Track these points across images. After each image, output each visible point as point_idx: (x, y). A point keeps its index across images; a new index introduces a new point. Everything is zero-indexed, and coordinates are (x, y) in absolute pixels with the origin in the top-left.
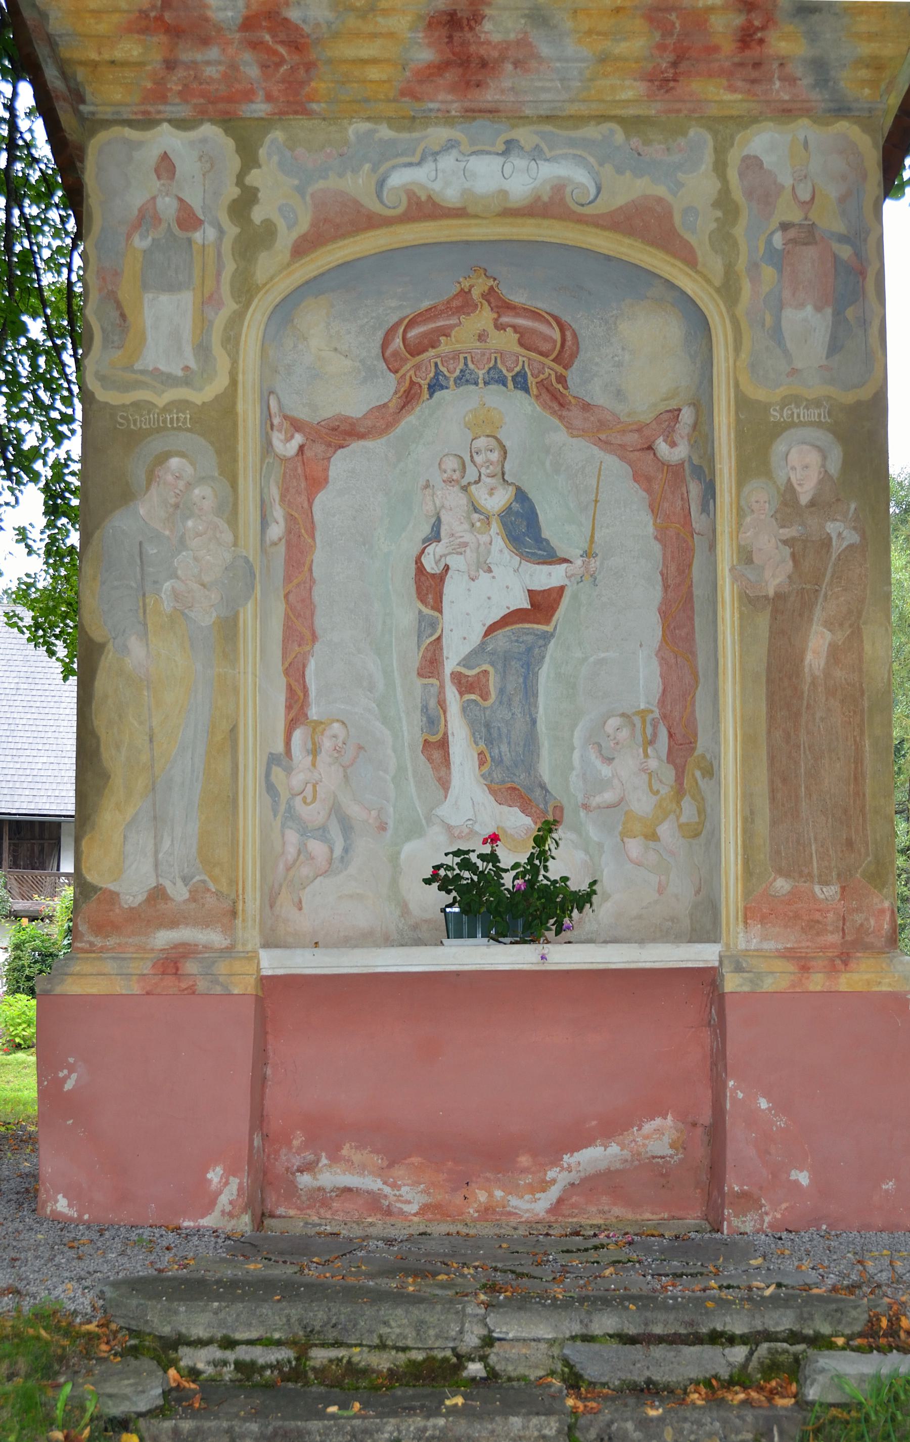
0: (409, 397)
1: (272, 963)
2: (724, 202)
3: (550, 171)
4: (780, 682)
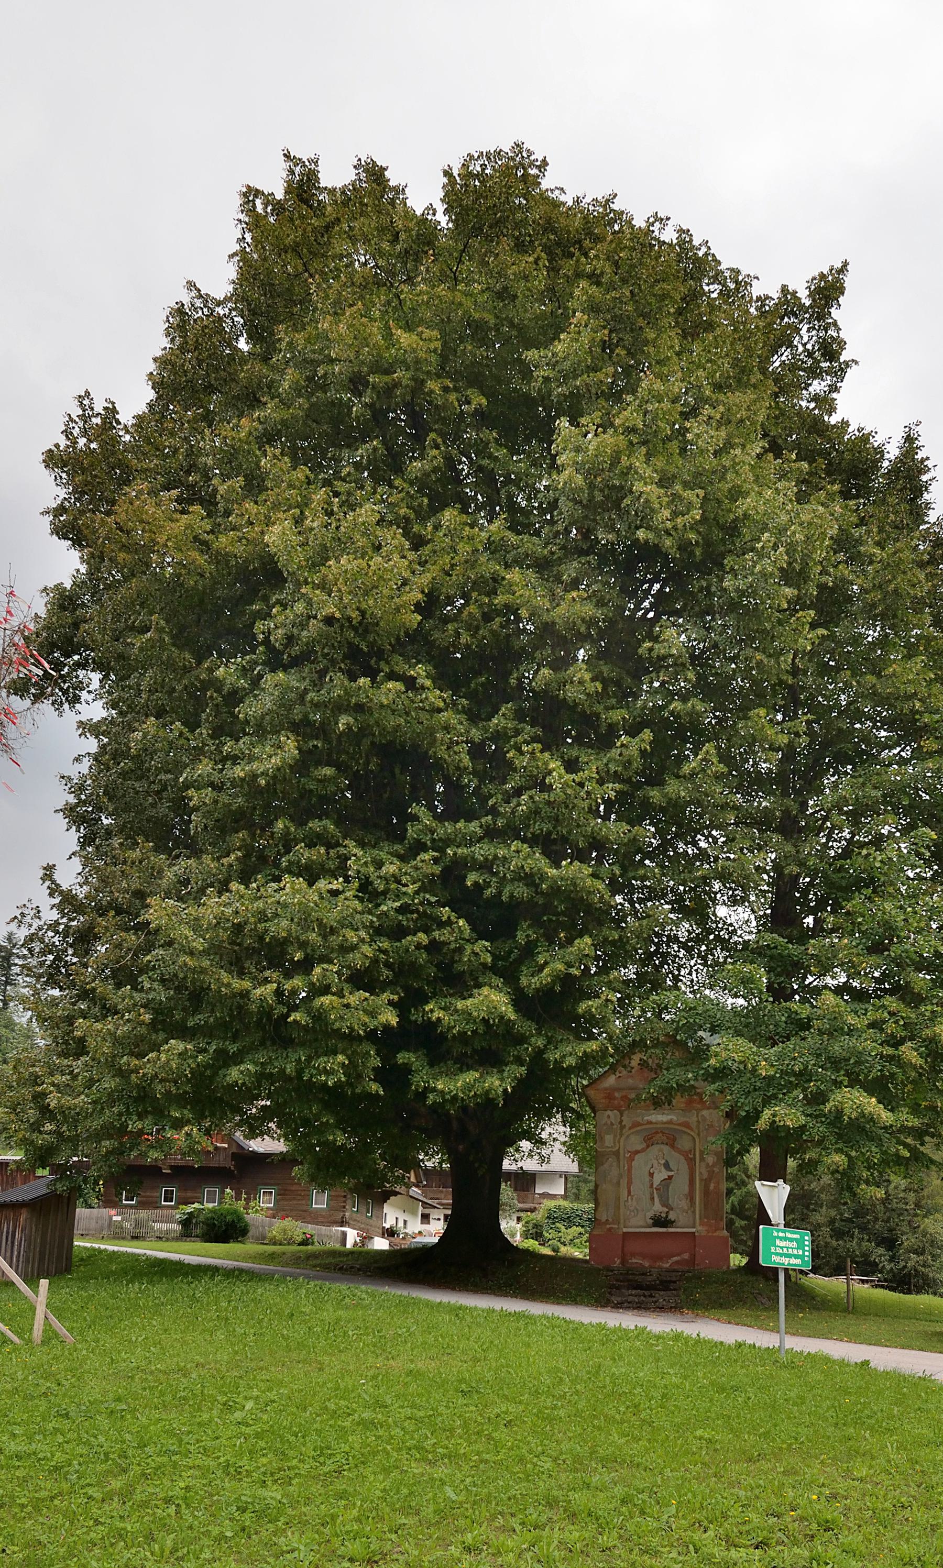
0: (648, 1147)
1: (625, 1230)
2: (698, 1122)
3: (670, 1117)
4: (706, 1192)
